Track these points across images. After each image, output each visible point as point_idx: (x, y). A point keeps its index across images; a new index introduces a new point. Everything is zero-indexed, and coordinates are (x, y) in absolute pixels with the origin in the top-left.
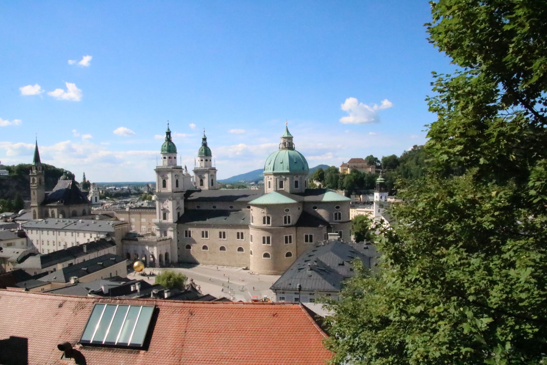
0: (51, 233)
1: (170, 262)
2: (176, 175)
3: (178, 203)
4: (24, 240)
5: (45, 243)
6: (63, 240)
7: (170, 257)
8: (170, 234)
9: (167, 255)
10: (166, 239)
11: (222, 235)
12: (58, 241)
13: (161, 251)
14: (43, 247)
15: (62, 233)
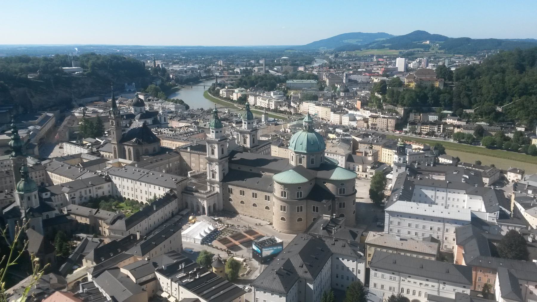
0: (130, 181)
1: (217, 209)
2: (221, 146)
3: (223, 166)
4: (110, 183)
5: (126, 188)
6: (139, 188)
7: (217, 206)
8: (217, 190)
9: (214, 205)
10: (214, 194)
11: (254, 195)
12: (135, 188)
13: (210, 204)
14: (124, 190)
15: (138, 183)
